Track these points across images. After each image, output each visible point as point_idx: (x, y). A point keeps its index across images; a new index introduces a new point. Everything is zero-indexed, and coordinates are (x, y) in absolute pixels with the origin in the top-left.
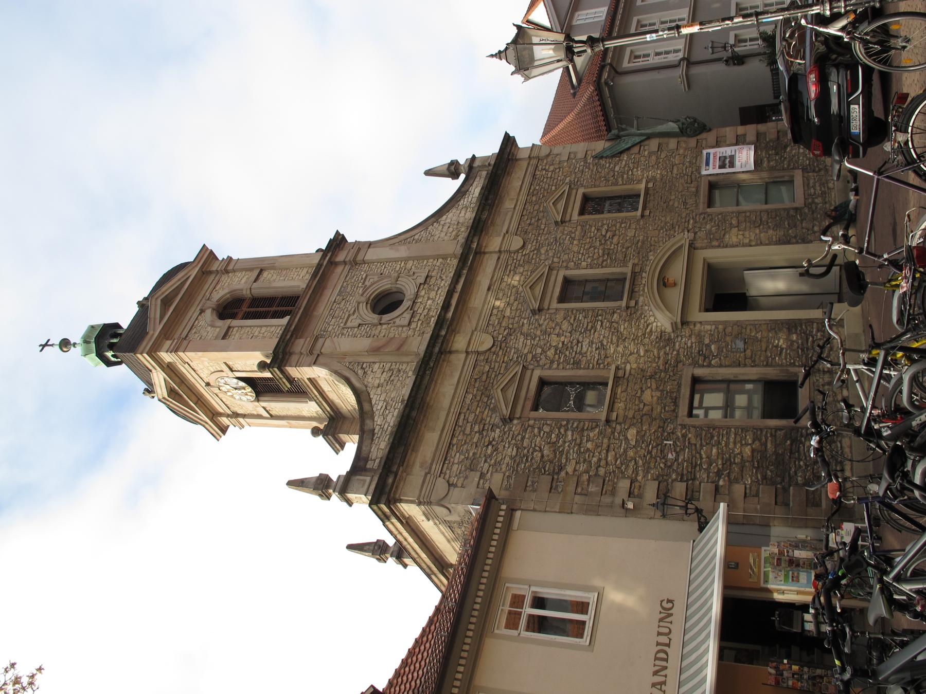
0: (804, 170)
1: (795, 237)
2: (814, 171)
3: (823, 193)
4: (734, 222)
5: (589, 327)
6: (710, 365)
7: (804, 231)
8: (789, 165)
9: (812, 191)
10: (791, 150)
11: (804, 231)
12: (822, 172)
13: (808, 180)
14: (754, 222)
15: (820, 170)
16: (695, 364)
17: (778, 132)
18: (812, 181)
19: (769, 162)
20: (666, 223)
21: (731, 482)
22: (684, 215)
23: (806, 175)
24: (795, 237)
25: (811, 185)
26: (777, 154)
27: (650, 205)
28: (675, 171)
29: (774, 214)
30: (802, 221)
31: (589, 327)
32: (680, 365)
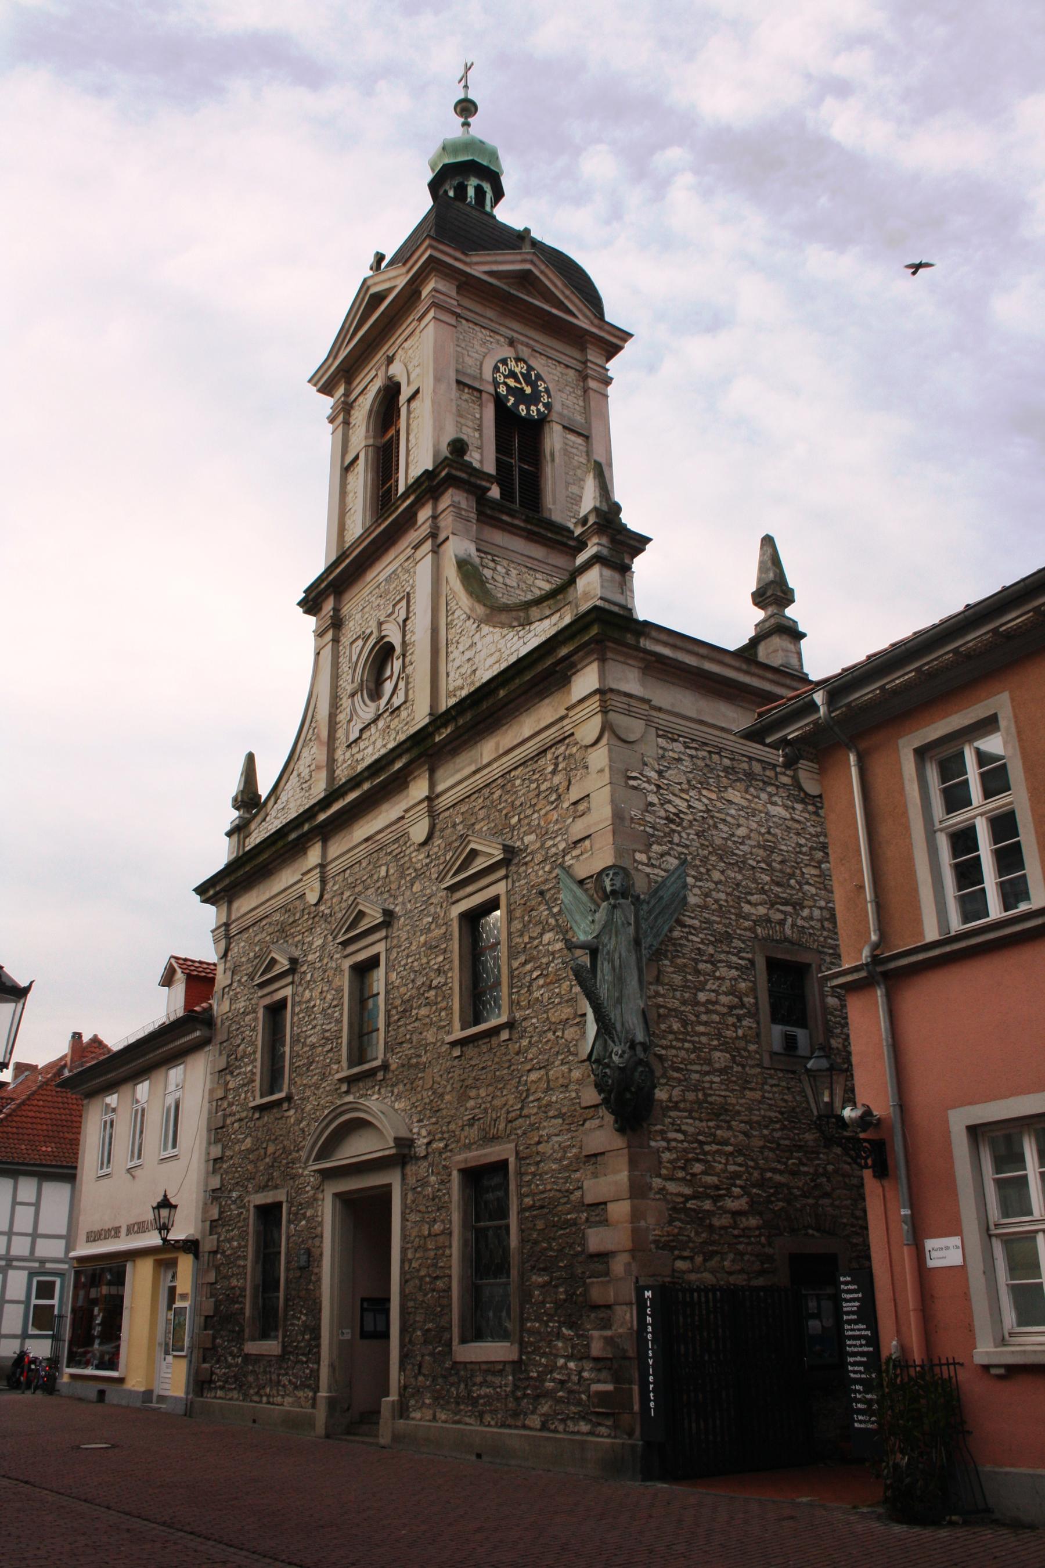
0: (518, 1366)
1: (410, 1341)
2: (516, 1387)
3: (474, 1402)
4: (438, 1227)
5: (327, 1034)
6: (289, 1222)
7: (419, 1358)
8: (531, 1332)
9: (479, 1379)
10: (566, 1339)
11: (419, 1358)
12: (511, 1405)
13: (500, 1372)
14: (435, 1265)
15: (517, 1399)
16: (290, 1203)
17: (608, 1307)
18: (497, 1380)
19: (543, 1286)
20: (442, 1095)
21: (217, 1268)
22: (452, 1126)
23: (509, 1368)
24: (410, 1341)
25: (489, 1378)
26: (558, 1305)
27: (470, 1051)
28: (534, 1076)
29: (445, 1301)
30: (432, 1354)
31: (327, 1034)
32: (291, 1182)
